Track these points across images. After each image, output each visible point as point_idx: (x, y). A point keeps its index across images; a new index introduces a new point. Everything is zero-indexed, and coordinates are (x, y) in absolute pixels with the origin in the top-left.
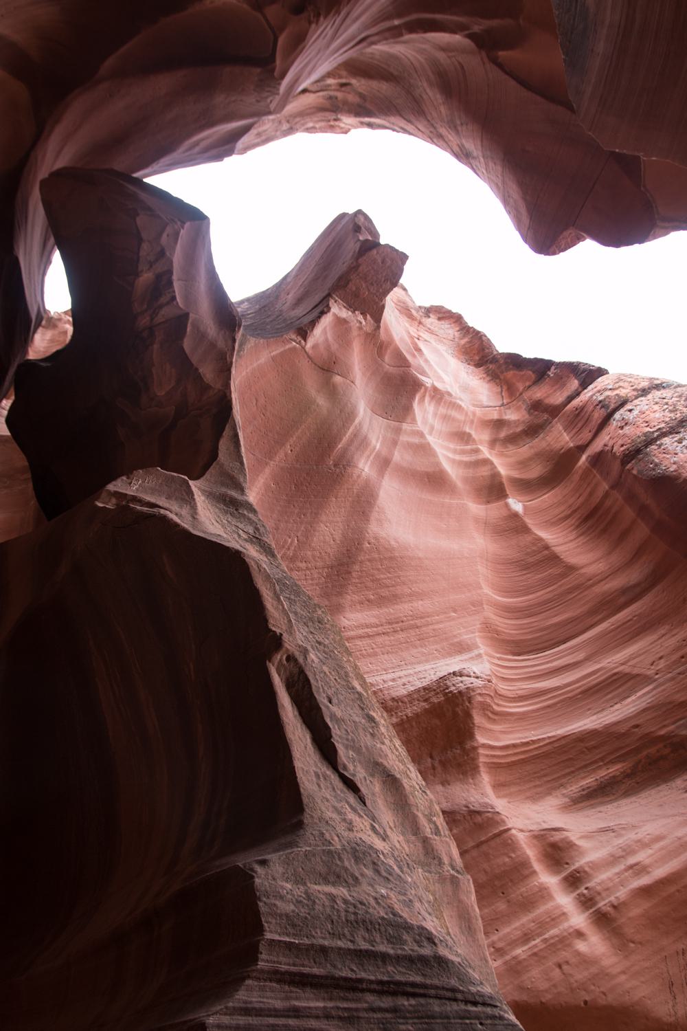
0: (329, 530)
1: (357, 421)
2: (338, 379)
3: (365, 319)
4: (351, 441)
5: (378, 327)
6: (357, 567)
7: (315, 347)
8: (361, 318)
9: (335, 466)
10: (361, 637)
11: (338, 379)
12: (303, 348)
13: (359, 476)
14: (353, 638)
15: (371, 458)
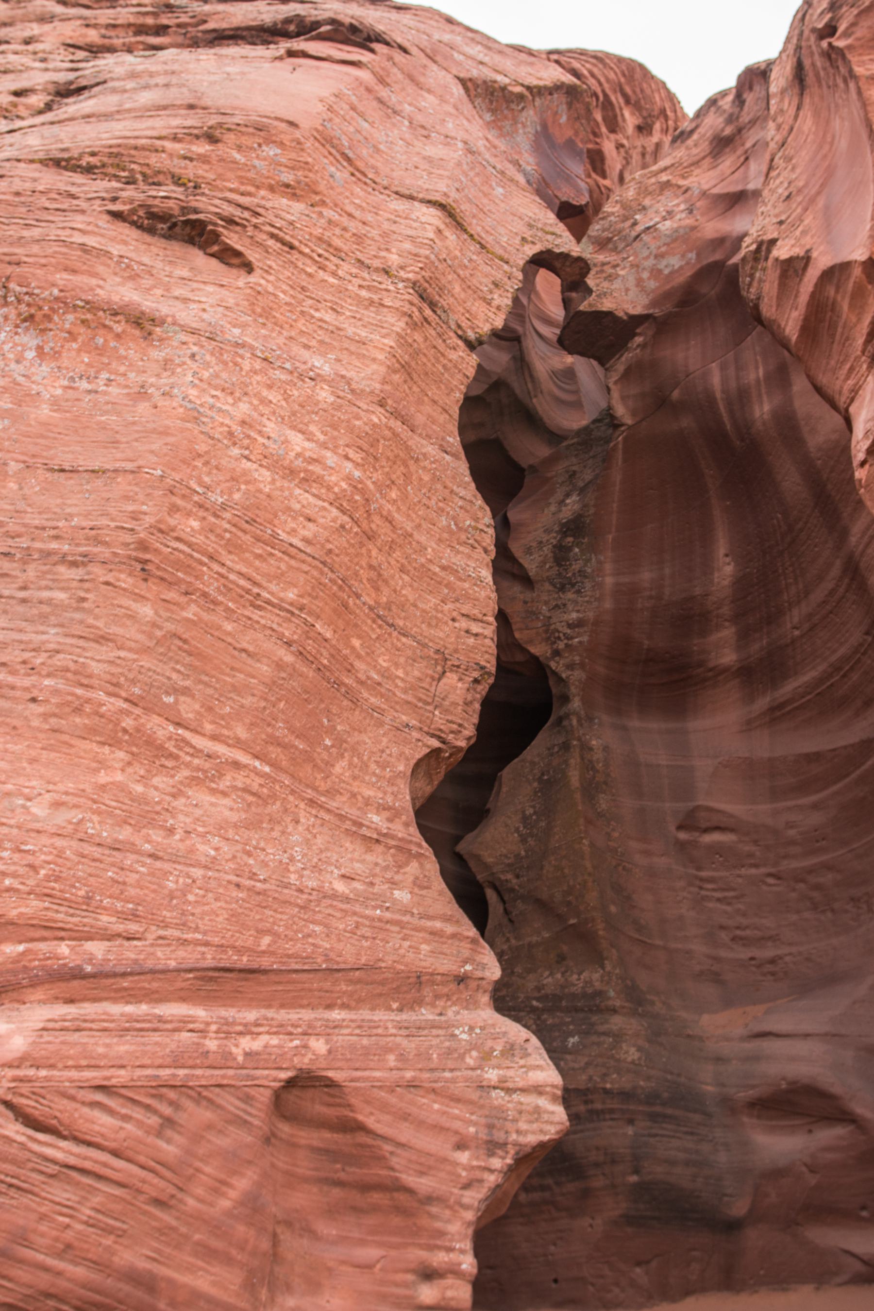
0: (790, 480)
1: (718, 395)
2: (676, 394)
3: (640, 334)
4: (731, 412)
5: (655, 318)
6: (829, 486)
7: (634, 414)
8: (639, 340)
9: (742, 440)
10: (868, 545)
11: (676, 394)
12: (630, 427)
13: (764, 424)
14: (864, 551)
15: (763, 391)
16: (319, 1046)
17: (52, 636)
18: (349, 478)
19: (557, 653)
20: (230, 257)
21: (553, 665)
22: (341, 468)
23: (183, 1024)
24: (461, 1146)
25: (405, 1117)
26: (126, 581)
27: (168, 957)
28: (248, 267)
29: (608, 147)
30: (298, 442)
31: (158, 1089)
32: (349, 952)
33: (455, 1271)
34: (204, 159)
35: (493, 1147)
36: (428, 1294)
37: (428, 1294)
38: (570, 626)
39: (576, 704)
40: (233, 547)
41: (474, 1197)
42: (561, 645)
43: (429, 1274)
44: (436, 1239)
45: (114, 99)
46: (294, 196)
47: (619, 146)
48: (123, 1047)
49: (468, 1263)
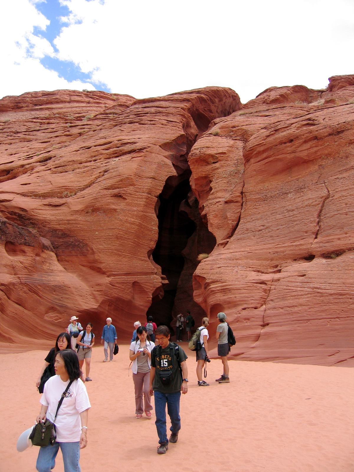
16: (137, 279)
17: (110, 246)
18: (139, 222)
19: (195, 219)
20: (125, 199)
21: (195, 221)
22: (138, 221)
23: (124, 278)
24: (151, 287)
25: (145, 285)
26: (116, 240)
27: (122, 273)
28: (126, 199)
29: (213, 108)
30: (132, 220)
31: (122, 283)
32: (140, 271)
33: (150, 297)
34: (121, 184)
35: (154, 287)
36: (148, 299)
37: (148, 299)
38: (198, 214)
39: (198, 228)
40: (126, 234)
41: (152, 292)
42: (196, 218)
43: (148, 298)
44: (149, 295)
45: (110, 174)
46: (132, 186)
47: (215, 106)
48: (119, 280)
49: (152, 297)
